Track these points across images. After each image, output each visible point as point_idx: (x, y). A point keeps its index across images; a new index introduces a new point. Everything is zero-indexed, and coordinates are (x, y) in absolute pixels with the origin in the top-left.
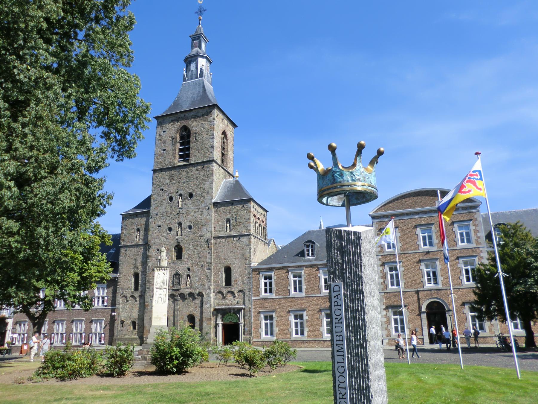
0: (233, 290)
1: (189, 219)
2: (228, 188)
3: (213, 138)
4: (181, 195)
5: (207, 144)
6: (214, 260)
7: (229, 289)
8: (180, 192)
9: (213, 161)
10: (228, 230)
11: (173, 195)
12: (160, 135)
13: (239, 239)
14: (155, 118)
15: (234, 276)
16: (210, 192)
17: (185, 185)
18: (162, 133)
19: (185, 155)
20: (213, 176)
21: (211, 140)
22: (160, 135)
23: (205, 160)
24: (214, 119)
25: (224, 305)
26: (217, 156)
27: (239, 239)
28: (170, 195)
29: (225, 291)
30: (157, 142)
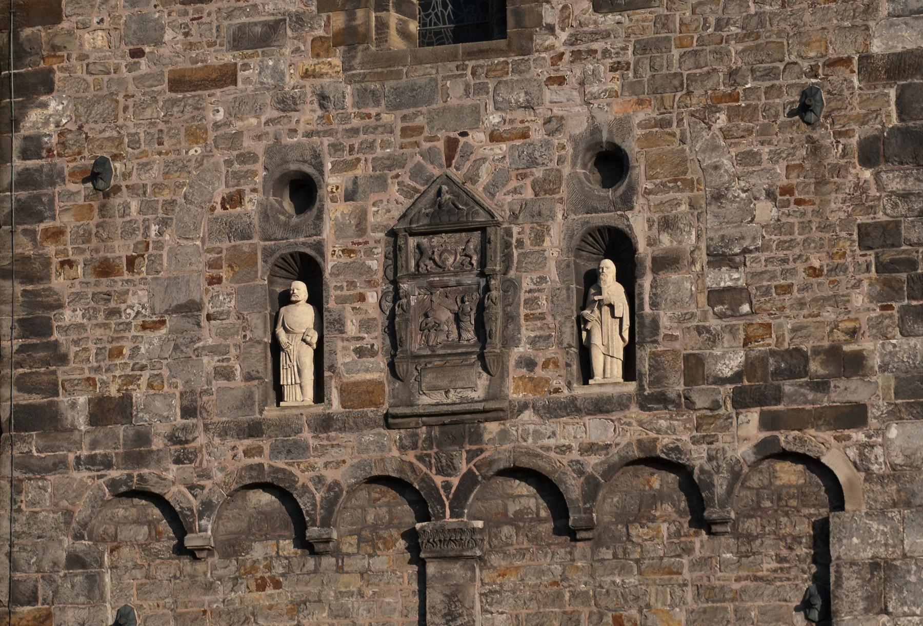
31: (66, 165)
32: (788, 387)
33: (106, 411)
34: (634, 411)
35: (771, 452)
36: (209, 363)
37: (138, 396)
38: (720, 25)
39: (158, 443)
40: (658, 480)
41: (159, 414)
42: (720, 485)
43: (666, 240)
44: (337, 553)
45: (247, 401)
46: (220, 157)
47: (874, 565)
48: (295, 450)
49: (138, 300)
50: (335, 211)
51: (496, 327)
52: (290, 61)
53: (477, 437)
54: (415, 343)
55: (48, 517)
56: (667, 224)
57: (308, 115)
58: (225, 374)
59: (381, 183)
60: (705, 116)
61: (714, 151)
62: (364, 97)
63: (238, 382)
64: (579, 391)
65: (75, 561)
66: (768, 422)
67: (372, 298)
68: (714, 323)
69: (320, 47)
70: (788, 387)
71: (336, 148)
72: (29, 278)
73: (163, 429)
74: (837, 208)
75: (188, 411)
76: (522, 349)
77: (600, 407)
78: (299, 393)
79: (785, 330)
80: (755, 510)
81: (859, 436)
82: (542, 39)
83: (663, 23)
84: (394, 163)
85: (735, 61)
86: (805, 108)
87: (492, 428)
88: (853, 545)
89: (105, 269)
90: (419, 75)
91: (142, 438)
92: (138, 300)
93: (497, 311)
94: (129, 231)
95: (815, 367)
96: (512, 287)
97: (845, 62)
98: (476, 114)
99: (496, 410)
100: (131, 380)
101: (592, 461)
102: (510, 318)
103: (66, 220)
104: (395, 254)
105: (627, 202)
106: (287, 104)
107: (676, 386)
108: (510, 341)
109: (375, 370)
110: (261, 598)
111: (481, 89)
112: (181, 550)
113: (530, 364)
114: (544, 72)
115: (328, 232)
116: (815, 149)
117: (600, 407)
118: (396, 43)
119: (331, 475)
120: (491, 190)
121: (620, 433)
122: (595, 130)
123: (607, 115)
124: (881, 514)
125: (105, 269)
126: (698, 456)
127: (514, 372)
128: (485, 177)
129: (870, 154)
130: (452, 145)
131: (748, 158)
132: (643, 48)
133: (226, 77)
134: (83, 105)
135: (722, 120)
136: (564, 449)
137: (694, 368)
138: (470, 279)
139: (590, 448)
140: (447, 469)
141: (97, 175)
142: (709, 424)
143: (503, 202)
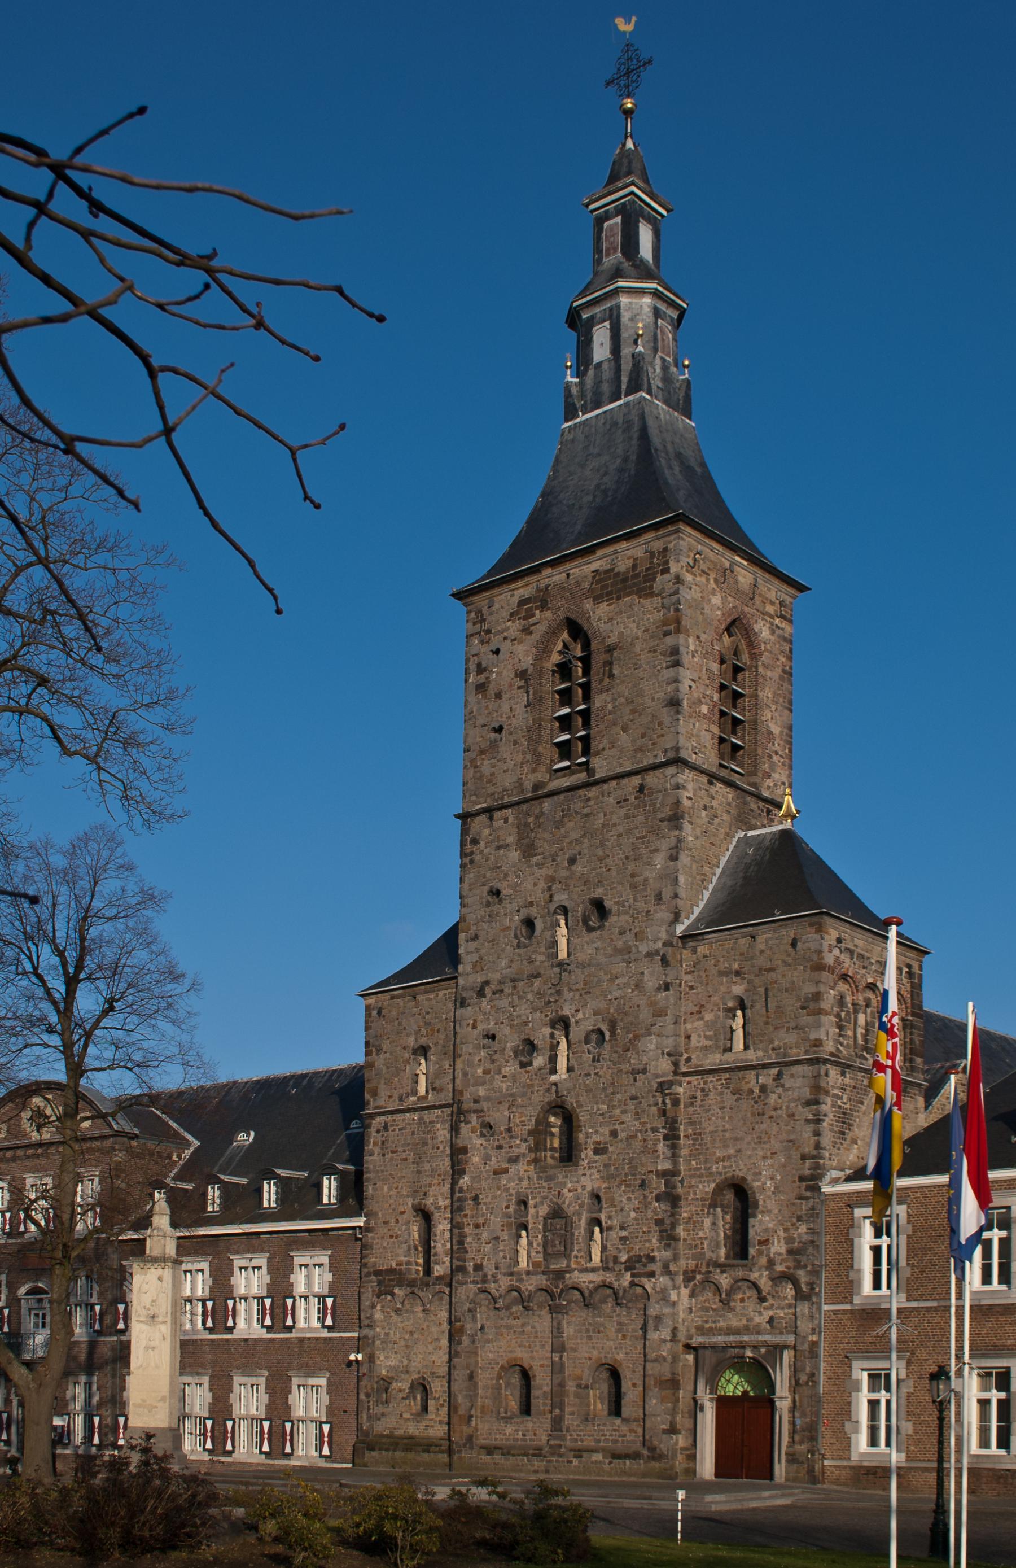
0: (754, 1276)
1: (592, 1004)
2: (748, 866)
3: (677, 664)
4: (565, 911)
5: (654, 693)
6: (688, 1162)
7: (740, 1273)
8: (561, 898)
9: (679, 762)
10: (739, 1043)
11: (534, 911)
12: (480, 670)
13: (779, 1076)
14: (458, 596)
15: (759, 1224)
16: (667, 894)
17: (578, 868)
18: (487, 659)
19: (577, 744)
20: (679, 828)
21: (670, 673)
22: (480, 670)
23: (648, 760)
24: (678, 580)
25: (720, 1331)
26: (698, 737)
27: (779, 1076)
28: (524, 912)
29: (724, 1280)
30: (472, 699)
31: (469, 1196)
32: (637, 1265)
33: (478, 1267)
34: (601, 1272)
35: (633, 1284)
36: (501, 1254)
37: (484, 1263)
38: (624, 1160)
39: (489, 1277)
40: (609, 1291)
41: (489, 1269)
42: (621, 1293)
43: (609, 1222)
44: (532, 1310)
45: (510, 1266)
46: (504, 1194)
47: (656, 1317)
48: (521, 1280)
49: (485, 1236)
50: (532, 1211)
51: (569, 1246)
52: (522, 1168)
53: (564, 1278)
54: (550, 1250)
55: (463, 1297)
56: (610, 1218)
57: (525, 1183)
58: (505, 1258)
59: (542, 1203)
60: (619, 1186)
61: (621, 1196)
62: (539, 1178)
63: (508, 1260)
64: (589, 1265)
65: (470, 1310)
66: (633, 1275)
67: (540, 1236)
68: (620, 1247)
69: (529, 1163)
70: (637, 1265)
71: (532, 1193)
72: (460, 1228)
73: (490, 1273)
74: (650, 1214)
75: (497, 1268)
76: (575, 1253)
77: (593, 1270)
78: (523, 1263)
79: (637, 1249)
80: (631, 1301)
81: (653, 1280)
82: (581, 1163)
83: (610, 1158)
84: (545, 1198)
85: (627, 1171)
86: (643, 1185)
87: (568, 1275)
88: (652, 1312)
89: (477, 1226)
90: (551, 1172)
91: (485, 1275)
92: (485, 1236)
93: (569, 1241)
94: (483, 1216)
95: (644, 1260)
96: (573, 1234)
97: (652, 1172)
98: (565, 1183)
99: (570, 1271)
100: (483, 1259)
101: (591, 1285)
102: (572, 1244)
103: (468, 1212)
104: (545, 1225)
105: (600, 1211)
106: (521, 1180)
107: (611, 1265)
108: (572, 1250)
109: (540, 1258)
110: (515, 1322)
111: (566, 1177)
112: (495, 1308)
113: (577, 1257)
114: (581, 1172)
115: (530, 1218)
116: (645, 1197)
117: (593, 1270)
118: (550, 1161)
119: (530, 1288)
120: (568, 1206)
121: (597, 1278)
122: (593, 1189)
123: (596, 1186)
124: (658, 1302)
125: (477, 1226)
126: (616, 1285)
127: (573, 1259)
128: (567, 1203)
129: (658, 1199)
130: (559, 1192)
131: (629, 1199)
132: (605, 1166)
133: (506, 1171)
134: (473, 1179)
135: (623, 1187)
136: (584, 1282)
137: (616, 1260)
138: (563, 1232)
139: (590, 1282)
140: (557, 1287)
141: (476, 1198)
142: (619, 1276)
143: (570, 1210)
